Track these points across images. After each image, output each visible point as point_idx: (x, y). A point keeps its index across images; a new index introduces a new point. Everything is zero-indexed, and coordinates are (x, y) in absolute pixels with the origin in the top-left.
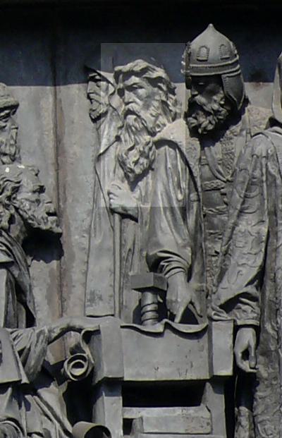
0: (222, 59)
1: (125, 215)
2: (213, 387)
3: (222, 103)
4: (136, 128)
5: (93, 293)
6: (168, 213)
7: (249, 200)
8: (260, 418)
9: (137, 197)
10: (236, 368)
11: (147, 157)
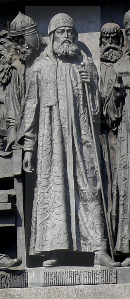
0: (23, 28)
2: (17, 181)
3: (27, 47)
7: (31, 92)
9: (6, 93)
10: (23, 171)
11: (8, 75)
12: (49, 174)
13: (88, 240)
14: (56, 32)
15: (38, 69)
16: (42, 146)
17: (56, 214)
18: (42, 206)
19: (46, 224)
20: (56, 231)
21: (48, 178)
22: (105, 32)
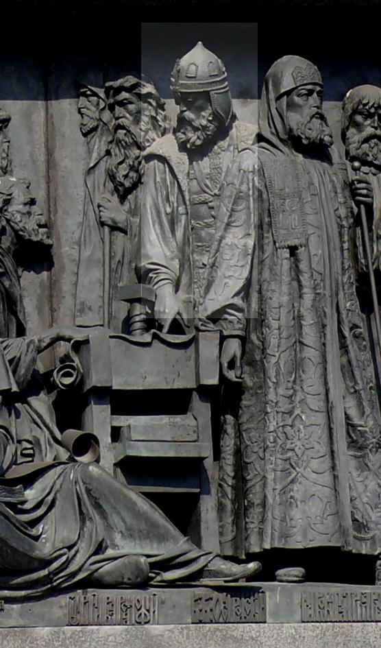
0: (210, 76)
1: (114, 228)
2: (200, 398)
3: (210, 118)
4: (126, 143)
5: (82, 303)
6: (157, 226)
7: (237, 213)
8: (245, 427)
10: (222, 377)
11: (137, 171)
12: (293, 388)
13: (368, 530)
14: (294, 92)
15: (254, 166)
16: (277, 328)
17: (314, 472)
18: (282, 454)
19: (290, 492)
20: (314, 508)
21: (291, 396)
22: (368, 103)
